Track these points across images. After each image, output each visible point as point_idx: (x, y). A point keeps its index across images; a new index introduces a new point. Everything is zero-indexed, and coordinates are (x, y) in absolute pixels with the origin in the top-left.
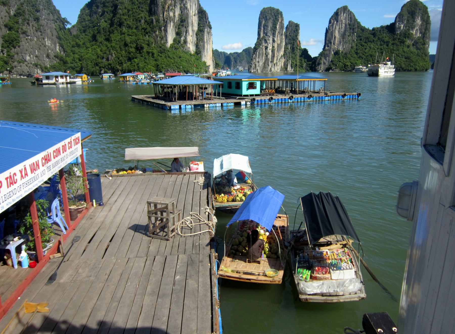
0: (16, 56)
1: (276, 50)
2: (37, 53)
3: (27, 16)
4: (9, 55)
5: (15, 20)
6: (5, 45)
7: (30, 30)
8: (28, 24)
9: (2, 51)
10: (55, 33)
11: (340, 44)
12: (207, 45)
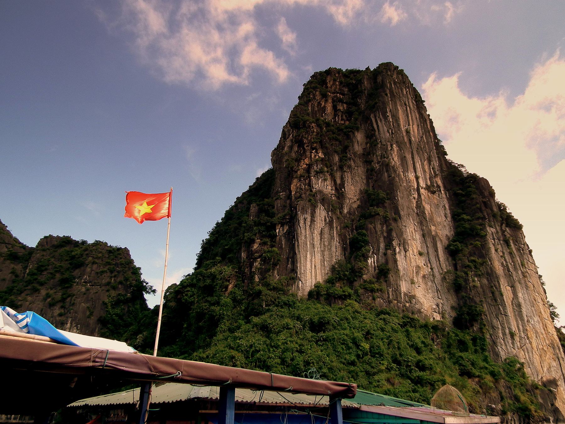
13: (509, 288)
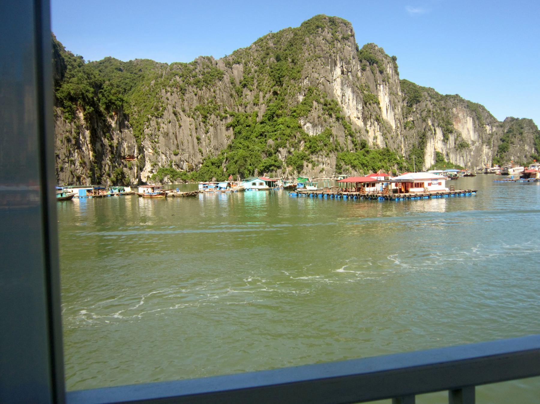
0: (505, 157)
2: (518, 155)
3: (515, 132)
4: (501, 157)
5: (507, 135)
6: (499, 151)
7: (516, 140)
8: (515, 137)
9: (497, 155)
10: (532, 141)
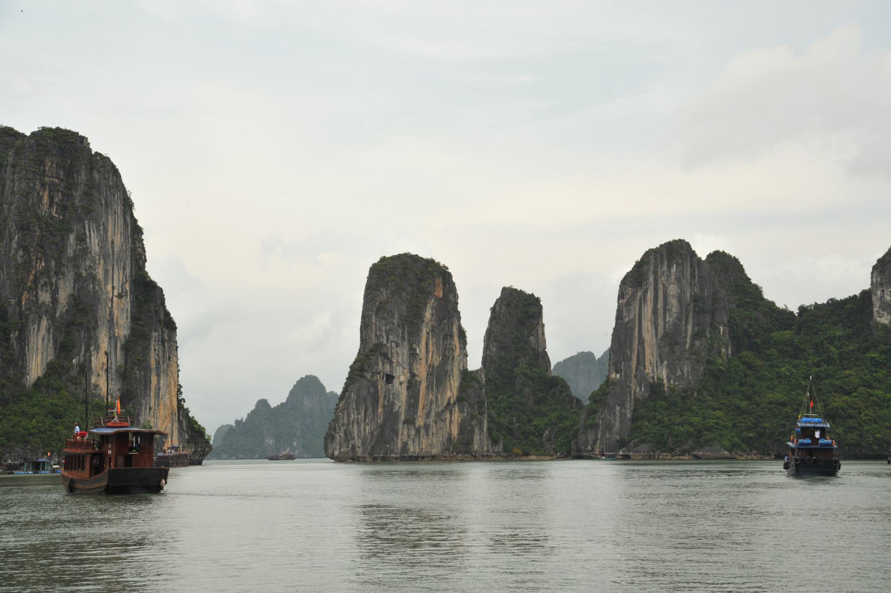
1: (423, 386)
11: (662, 362)
12: (158, 376)
13: (156, 377)
